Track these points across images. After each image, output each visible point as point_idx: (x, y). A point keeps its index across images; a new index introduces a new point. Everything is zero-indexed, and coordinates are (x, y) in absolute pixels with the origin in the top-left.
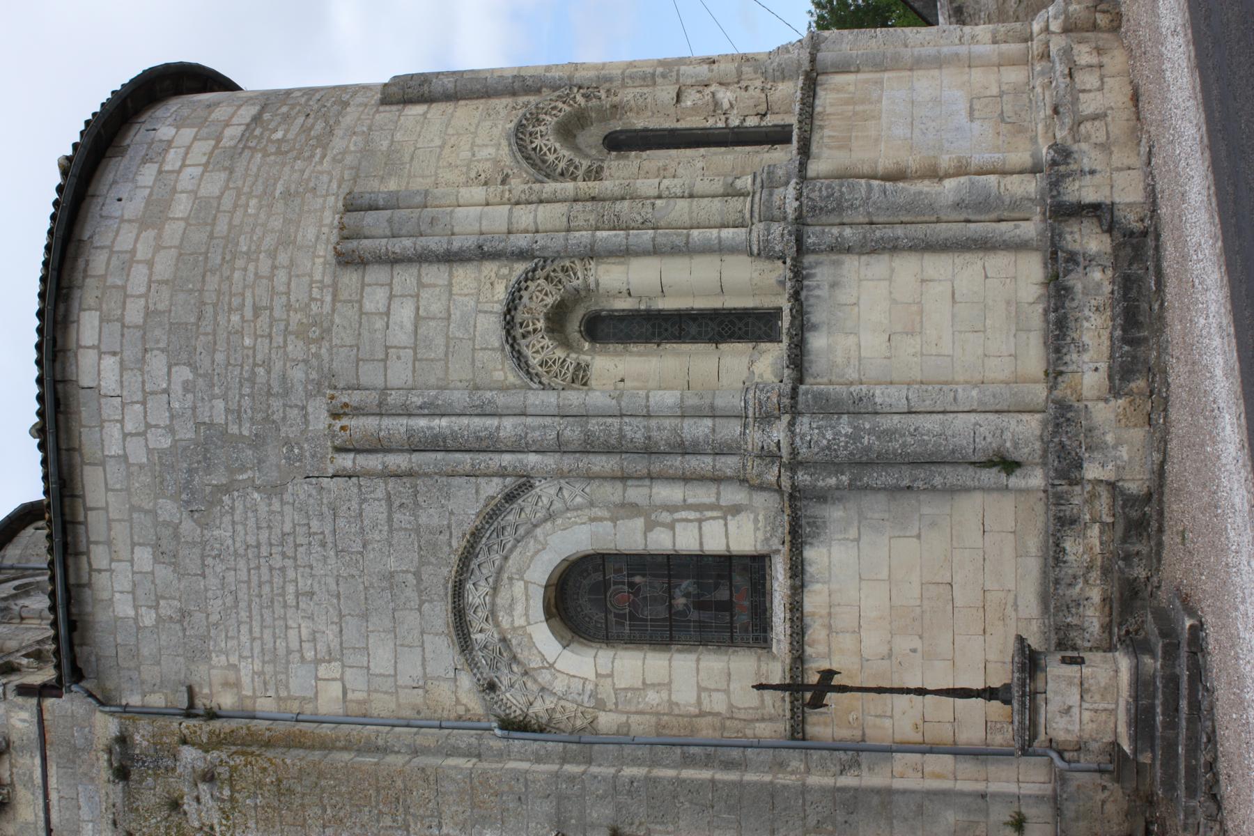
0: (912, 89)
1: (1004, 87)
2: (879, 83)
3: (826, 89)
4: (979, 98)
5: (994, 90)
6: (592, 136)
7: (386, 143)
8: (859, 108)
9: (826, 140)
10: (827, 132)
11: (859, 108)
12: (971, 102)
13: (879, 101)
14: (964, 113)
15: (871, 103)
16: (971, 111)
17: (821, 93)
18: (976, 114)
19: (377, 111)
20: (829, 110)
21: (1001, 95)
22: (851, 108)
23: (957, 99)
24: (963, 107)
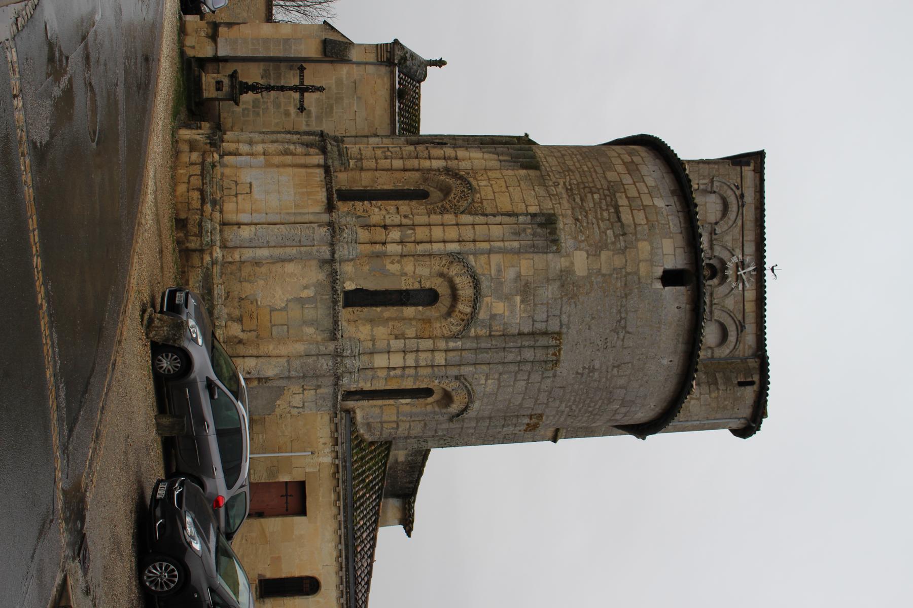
0: (280, 200)
1: (235, 199)
2: (297, 206)
3: (323, 202)
4: (247, 193)
5: (240, 197)
6: (436, 194)
7: (537, 190)
8: (305, 190)
9: (318, 176)
10: (318, 179)
11: (305, 190)
12: (251, 192)
13: (295, 194)
14: (254, 186)
15: (299, 193)
16: (250, 187)
17: (325, 200)
18: (248, 185)
19: (553, 209)
20: (319, 189)
21: (236, 195)
22: (308, 190)
23: (257, 194)
24: (255, 189)
